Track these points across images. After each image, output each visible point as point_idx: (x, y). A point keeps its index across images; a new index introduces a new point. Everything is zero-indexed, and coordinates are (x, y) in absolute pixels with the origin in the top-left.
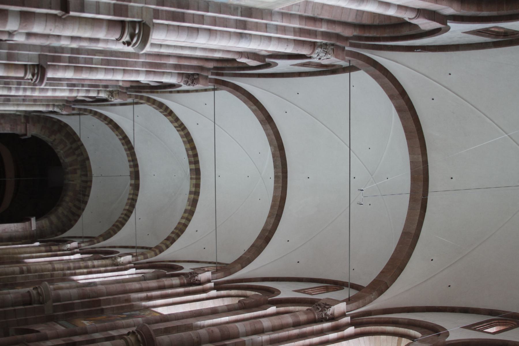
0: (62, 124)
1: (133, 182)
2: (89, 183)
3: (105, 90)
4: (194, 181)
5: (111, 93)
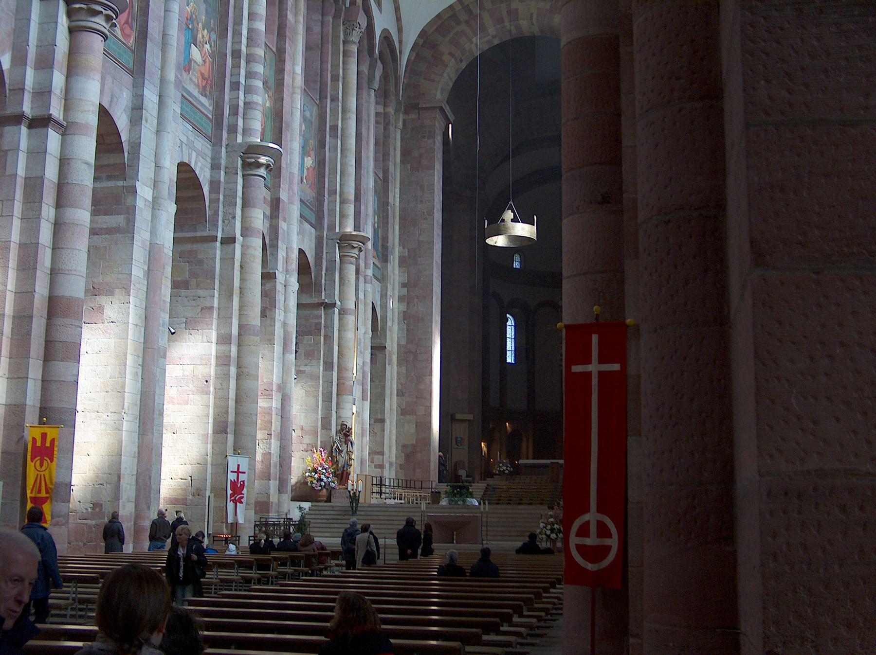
0: (421, 42)
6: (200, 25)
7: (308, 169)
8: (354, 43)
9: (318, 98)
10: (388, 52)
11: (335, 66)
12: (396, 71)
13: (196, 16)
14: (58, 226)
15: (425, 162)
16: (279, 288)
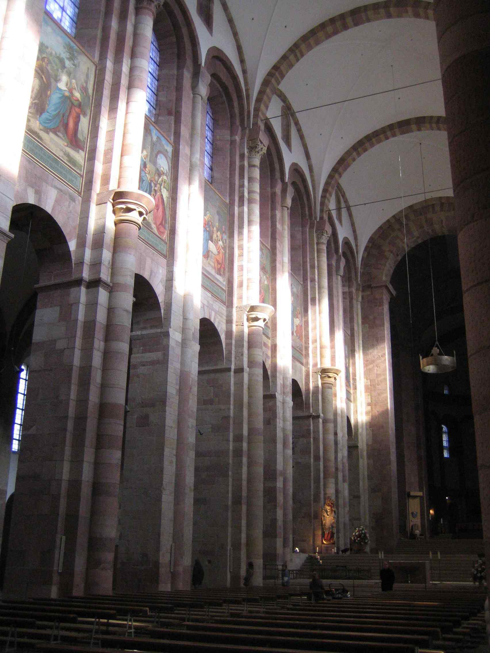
1: (414, 127)
2: (443, 201)
3: (249, 158)
4: (370, 13)
5: (252, 149)
6: (215, 229)
7: (297, 326)
8: (324, 244)
9: (302, 280)
10: (349, 254)
11: (312, 259)
12: (355, 264)
13: (212, 223)
14: (107, 355)
15: (377, 322)
16: (279, 404)
